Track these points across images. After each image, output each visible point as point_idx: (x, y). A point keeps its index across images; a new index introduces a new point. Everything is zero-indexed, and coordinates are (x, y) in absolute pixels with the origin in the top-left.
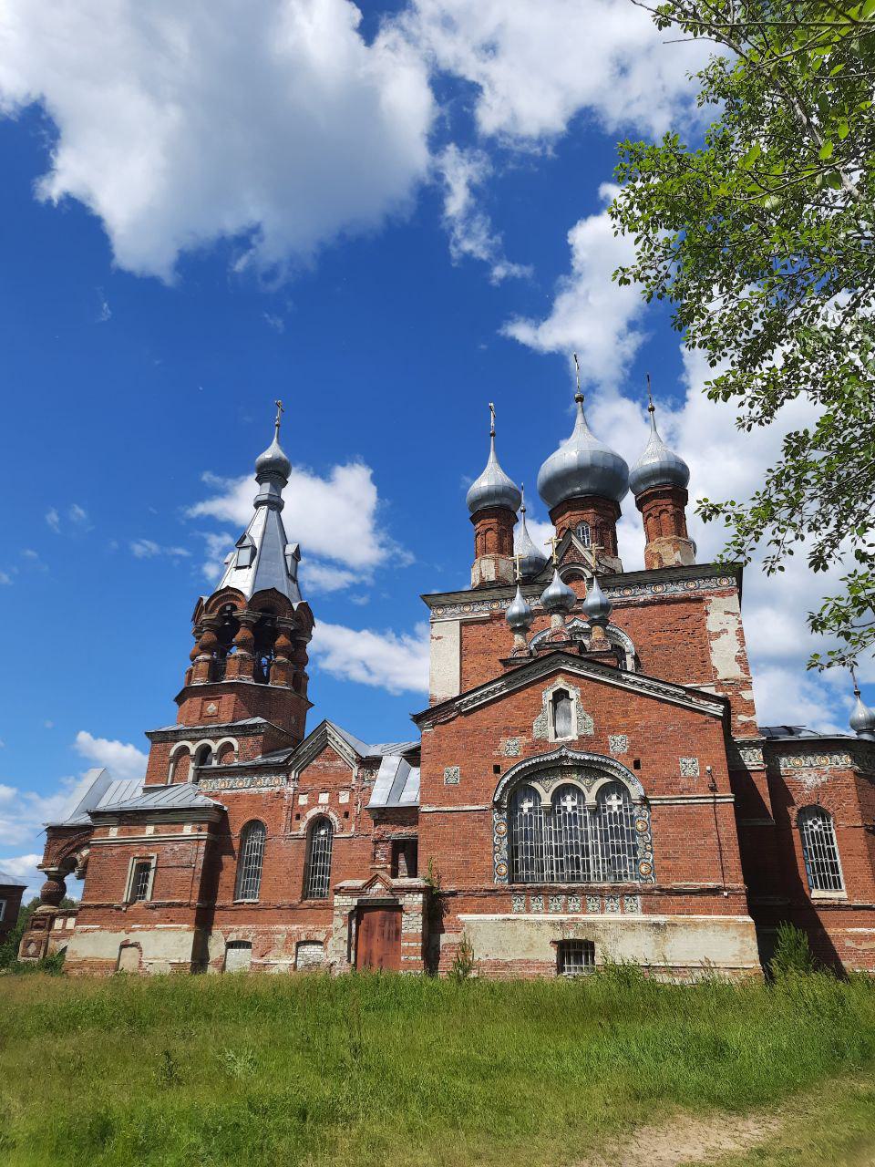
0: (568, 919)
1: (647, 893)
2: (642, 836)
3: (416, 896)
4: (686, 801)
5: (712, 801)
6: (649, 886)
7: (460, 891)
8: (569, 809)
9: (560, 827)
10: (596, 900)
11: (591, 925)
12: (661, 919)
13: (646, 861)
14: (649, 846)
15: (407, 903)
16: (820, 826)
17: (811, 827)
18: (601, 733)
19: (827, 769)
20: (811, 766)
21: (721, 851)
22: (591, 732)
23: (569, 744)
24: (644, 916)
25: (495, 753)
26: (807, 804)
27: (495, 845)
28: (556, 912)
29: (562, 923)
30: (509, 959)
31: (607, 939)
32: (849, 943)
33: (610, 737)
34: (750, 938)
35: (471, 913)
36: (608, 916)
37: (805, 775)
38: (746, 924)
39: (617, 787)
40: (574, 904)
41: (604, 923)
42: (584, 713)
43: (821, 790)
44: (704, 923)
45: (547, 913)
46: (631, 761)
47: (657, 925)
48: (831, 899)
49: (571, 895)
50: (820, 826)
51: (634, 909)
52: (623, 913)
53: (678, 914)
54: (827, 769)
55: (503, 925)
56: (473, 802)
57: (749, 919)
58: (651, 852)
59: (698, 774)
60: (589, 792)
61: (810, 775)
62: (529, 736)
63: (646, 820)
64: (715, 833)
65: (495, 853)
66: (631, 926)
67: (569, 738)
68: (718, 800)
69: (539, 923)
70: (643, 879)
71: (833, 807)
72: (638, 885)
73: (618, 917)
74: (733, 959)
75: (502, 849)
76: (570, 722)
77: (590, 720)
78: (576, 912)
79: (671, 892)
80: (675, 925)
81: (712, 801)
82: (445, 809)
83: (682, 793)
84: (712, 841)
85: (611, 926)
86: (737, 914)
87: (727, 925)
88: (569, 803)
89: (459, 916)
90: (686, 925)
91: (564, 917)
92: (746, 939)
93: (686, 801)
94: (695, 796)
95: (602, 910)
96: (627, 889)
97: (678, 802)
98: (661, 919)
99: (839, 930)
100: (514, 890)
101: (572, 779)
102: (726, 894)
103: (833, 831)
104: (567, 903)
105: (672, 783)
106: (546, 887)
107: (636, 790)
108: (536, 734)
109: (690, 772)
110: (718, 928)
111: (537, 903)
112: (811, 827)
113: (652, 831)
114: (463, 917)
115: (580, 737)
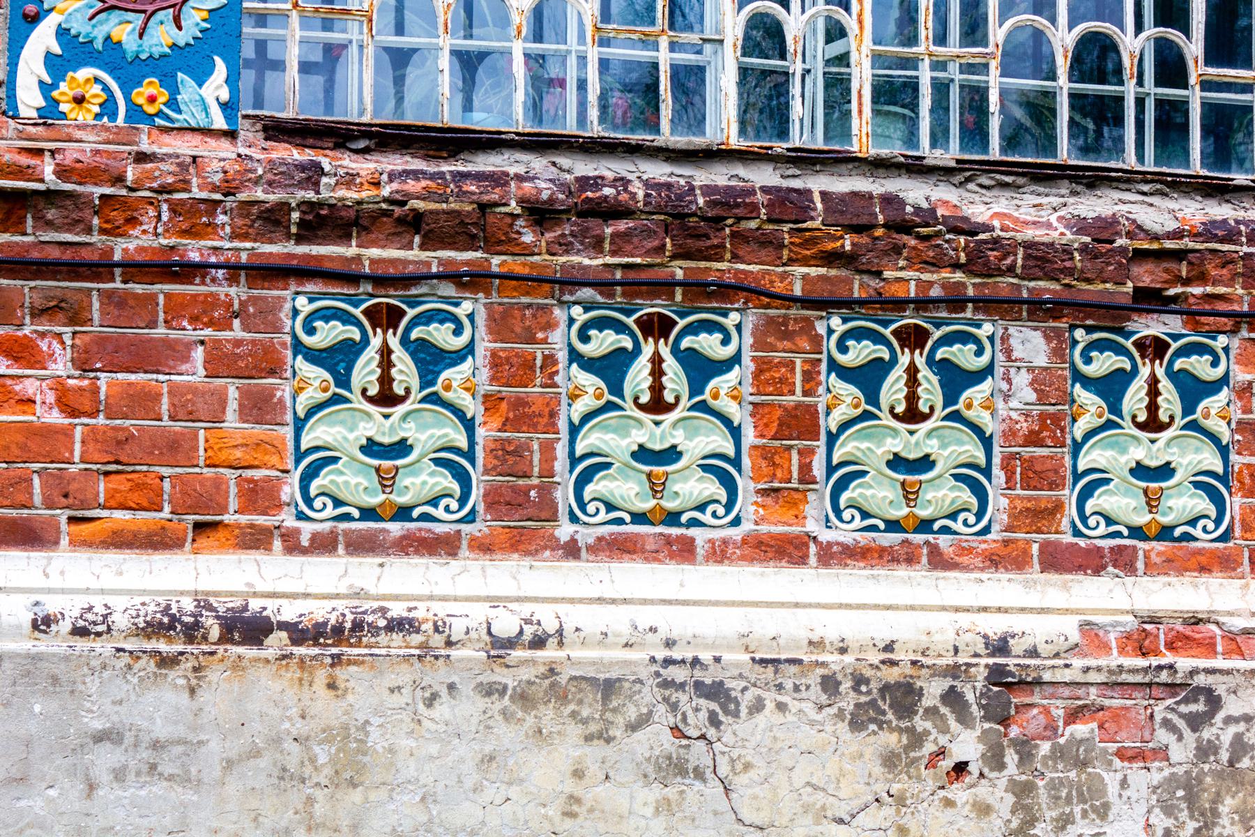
28: (912, 542)
29: (1007, 685)
45: (789, 550)
49: (1109, 318)
55: (160, 706)
69: (706, 692)
78: (1171, 546)
100: (324, 222)
104: (1049, 426)
106: (789, 205)
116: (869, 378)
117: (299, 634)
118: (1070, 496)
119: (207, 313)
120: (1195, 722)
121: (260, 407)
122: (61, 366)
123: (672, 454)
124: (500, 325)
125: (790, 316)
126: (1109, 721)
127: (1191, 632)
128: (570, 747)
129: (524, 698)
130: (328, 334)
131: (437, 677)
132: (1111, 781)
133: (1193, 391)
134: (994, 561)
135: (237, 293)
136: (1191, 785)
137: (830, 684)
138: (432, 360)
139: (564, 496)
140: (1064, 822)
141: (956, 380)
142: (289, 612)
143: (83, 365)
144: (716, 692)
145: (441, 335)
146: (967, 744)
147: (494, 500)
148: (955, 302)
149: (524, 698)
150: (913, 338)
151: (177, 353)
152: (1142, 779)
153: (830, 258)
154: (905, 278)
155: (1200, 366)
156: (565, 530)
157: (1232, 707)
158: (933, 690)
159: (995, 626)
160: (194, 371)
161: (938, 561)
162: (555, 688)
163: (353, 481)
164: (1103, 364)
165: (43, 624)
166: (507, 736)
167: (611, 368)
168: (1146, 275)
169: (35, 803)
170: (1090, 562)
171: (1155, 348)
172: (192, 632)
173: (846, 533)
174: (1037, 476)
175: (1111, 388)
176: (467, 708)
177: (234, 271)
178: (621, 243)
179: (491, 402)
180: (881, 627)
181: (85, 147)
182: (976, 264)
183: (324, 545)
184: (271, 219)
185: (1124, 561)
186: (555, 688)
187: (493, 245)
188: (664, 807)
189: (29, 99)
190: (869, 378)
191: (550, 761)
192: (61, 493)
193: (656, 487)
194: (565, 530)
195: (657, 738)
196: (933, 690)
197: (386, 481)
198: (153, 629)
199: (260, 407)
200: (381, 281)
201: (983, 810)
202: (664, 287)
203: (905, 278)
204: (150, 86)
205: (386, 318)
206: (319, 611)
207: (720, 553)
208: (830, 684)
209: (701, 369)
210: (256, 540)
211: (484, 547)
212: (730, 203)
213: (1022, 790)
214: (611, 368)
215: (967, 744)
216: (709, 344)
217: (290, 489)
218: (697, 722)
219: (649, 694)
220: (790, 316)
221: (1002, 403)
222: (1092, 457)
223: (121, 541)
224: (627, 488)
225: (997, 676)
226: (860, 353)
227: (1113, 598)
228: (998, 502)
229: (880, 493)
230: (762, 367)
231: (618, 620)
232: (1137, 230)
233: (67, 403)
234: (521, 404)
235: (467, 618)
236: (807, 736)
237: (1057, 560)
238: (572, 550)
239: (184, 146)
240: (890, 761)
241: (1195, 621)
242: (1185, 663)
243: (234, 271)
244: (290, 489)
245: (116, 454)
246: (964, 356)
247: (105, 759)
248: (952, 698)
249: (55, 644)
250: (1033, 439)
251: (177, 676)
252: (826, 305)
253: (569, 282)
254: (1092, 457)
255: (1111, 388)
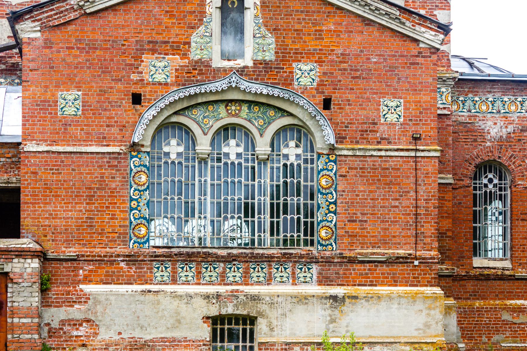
0: (227, 291)
1: (328, 261)
2: (326, 194)
3: (29, 261)
4: (383, 153)
5: (413, 154)
6: (328, 254)
7: (83, 256)
8: (233, 157)
9: (219, 179)
10: (262, 268)
11: (255, 298)
12: (339, 291)
13: (328, 224)
14: (333, 206)
15: (17, 270)
16: (495, 186)
17: (486, 186)
18: (286, 56)
19: (515, 117)
20: (499, 112)
21: (416, 214)
22: (270, 56)
23: (242, 71)
24: (320, 287)
25: (134, 77)
26: (487, 159)
27: (132, 200)
28: (211, 283)
29: (218, 296)
30: (148, 337)
31: (273, 314)
32: (506, 316)
33: (294, 65)
34: (438, 310)
35: (97, 283)
36: (277, 287)
37: (490, 123)
38: (436, 298)
39: (299, 131)
40: (234, 274)
41: (271, 296)
42: (263, 29)
43: (503, 143)
44: (390, 297)
45: (199, 284)
46: (320, 98)
47: (334, 298)
48: (494, 268)
49: (230, 262)
50: (495, 186)
51: (308, 279)
52: (294, 284)
53: (359, 285)
54: (515, 117)
55: (142, 298)
56: (102, 140)
57: (438, 290)
58: (335, 213)
59: (402, 120)
60: (261, 135)
61: (495, 124)
62: (185, 56)
63: (332, 174)
64: (412, 194)
65: (132, 209)
66: (303, 300)
67: (240, 63)
68: (419, 154)
69: (190, 296)
70: (322, 245)
71: (514, 163)
72: (315, 252)
73: (288, 289)
74: (415, 333)
75: (141, 204)
76: (242, 40)
77: (271, 40)
78: (236, 283)
79: (352, 261)
80: (355, 298)
81: (413, 154)
82: (60, 149)
83: (379, 143)
84: (408, 202)
85: (280, 299)
86: (426, 286)
87: (414, 297)
88: (233, 148)
89: (81, 286)
90: (367, 298)
91: (222, 289)
92: (432, 312)
93: (383, 153)
94: (396, 147)
95: (269, 280)
96: (301, 256)
97: (375, 153)
98: (339, 291)
99: (497, 302)
101: (242, 117)
102: (416, 263)
103: (509, 192)
104: (224, 272)
105: (368, 131)
106: (199, 253)
107: (324, 135)
108: (195, 54)
109: (392, 118)
110: (403, 301)
111: (186, 273)
112: (486, 186)
113: (339, 188)
114: (88, 288)
115: (256, 63)
116: (206, 268)
117: (154, 292)
118: (226, 279)
119: (146, 264)
120: (237, 299)
121: (151, 272)
122: (134, 269)
123: (188, 276)
124: (172, 265)
125: (199, 263)
126: (228, 299)
127: (237, 291)
128: (178, 301)
129: (173, 297)
130: (157, 266)
131: (166, 295)
132: (228, 304)
133: (238, 268)
134: (219, 285)
135: (149, 263)
136: (236, 305)
137: (201, 296)
138: (166, 268)
139: (178, 279)
140: (224, 308)
141: (215, 268)
142: (153, 290)
143: (136, 269)
144: (191, 296)
145: (167, 266)
146: (214, 301)
147: (172, 280)
148: (215, 261)
149: (173, 297)
150: (211, 264)
151: (144, 268)
152: (231, 304)
153: (203, 258)
154: (210, 259)
155: (239, 266)
156: (178, 282)
157: (240, 298)
158: (211, 296)
159: (217, 291)
160: (145, 270)
161: (213, 285)
162: (176, 296)
163: (159, 279)
164: (229, 266)
165: (132, 291)
166: (172, 300)
167: (182, 268)
168: (234, 258)
169: (132, 306)
170: (228, 284)
171: (234, 265)
172: (145, 292)
173: (205, 282)
174: (223, 277)
175: (230, 268)
176: (169, 298)
177: (149, 261)
178: (183, 257)
179: (171, 271)
180: (207, 291)
181: (136, 250)
182: (216, 257)
183: (157, 284)
184: (152, 256)
185: (231, 284)
186: (176, 296)
187: (172, 258)
188: (186, 307)
189: (131, 247)
190: (206, 268)
191: (176, 302)
192: (134, 280)
193: (187, 278)
194: (178, 282)
195: (186, 301)
196: (211, 296)
197: (162, 278)
198: (141, 292)
199: (151, 272)
200: (162, 261)
201: (216, 307)
202: (187, 261)
203: (210, 259)
204: (141, 245)
205: (162, 264)
206: (156, 290)
207: (192, 284)
208: (201, 296)
209: (191, 268)
210: (151, 284)
211: (171, 284)
212: (193, 253)
213: (220, 305)
214: (182, 268)
215: (214, 301)
216: (191, 266)
217: (154, 279)
218: (189, 299)
219: (185, 297)
220: (199, 263)
221: (220, 270)
222: (228, 275)
223: (139, 284)
224: (184, 279)
225: (217, 295)
226: (206, 266)
227: (230, 288)
228: (219, 279)
229: (208, 279)
230: (196, 267)
231: (182, 290)
232: (233, 254)
233: (135, 272)
234: (174, 272)
235: (168, 290)
236: (199, 300)
237: (225, 284)
238: (179, 284)
239: (144, 250)
240: (207, 303)
241: (238, 290)
242: (235, 294)
243: (149, 261)
244: (154, 279)
245: (139, 276)
246: (215, 266)
247: (138, 302)
248: (213, 297)
249: (133, 293)
250: (222, 273)
251: (144, 295)
252: (202, 262)
253: (178, 261)
254: (228, 275)
255: (230, 268)
